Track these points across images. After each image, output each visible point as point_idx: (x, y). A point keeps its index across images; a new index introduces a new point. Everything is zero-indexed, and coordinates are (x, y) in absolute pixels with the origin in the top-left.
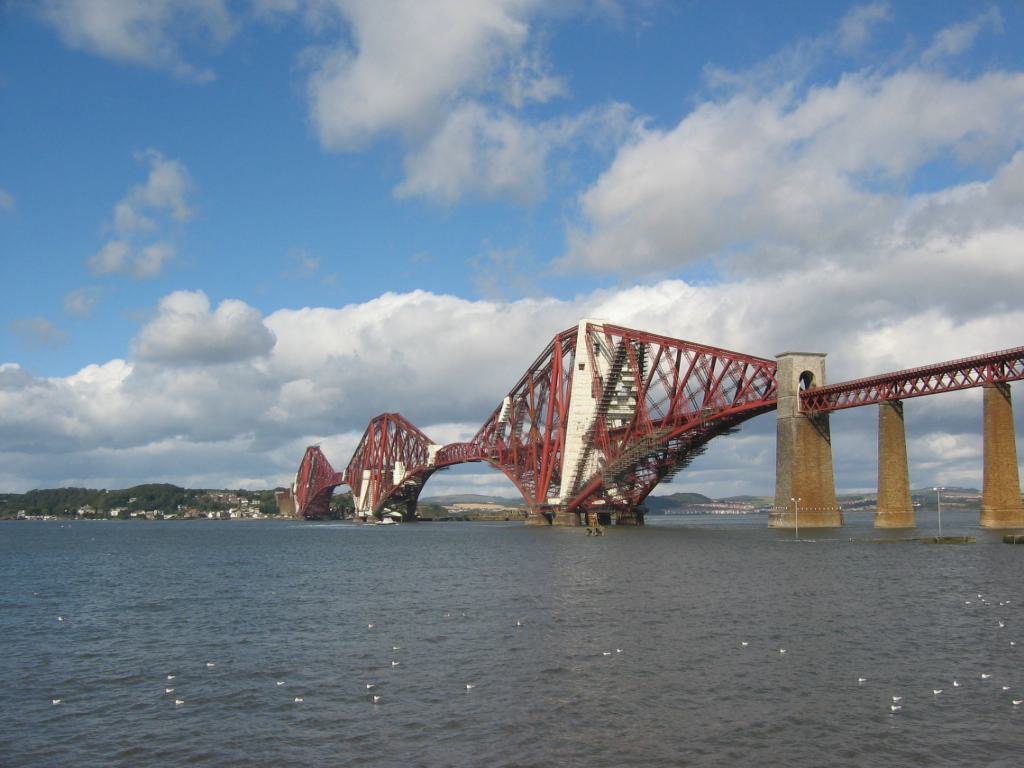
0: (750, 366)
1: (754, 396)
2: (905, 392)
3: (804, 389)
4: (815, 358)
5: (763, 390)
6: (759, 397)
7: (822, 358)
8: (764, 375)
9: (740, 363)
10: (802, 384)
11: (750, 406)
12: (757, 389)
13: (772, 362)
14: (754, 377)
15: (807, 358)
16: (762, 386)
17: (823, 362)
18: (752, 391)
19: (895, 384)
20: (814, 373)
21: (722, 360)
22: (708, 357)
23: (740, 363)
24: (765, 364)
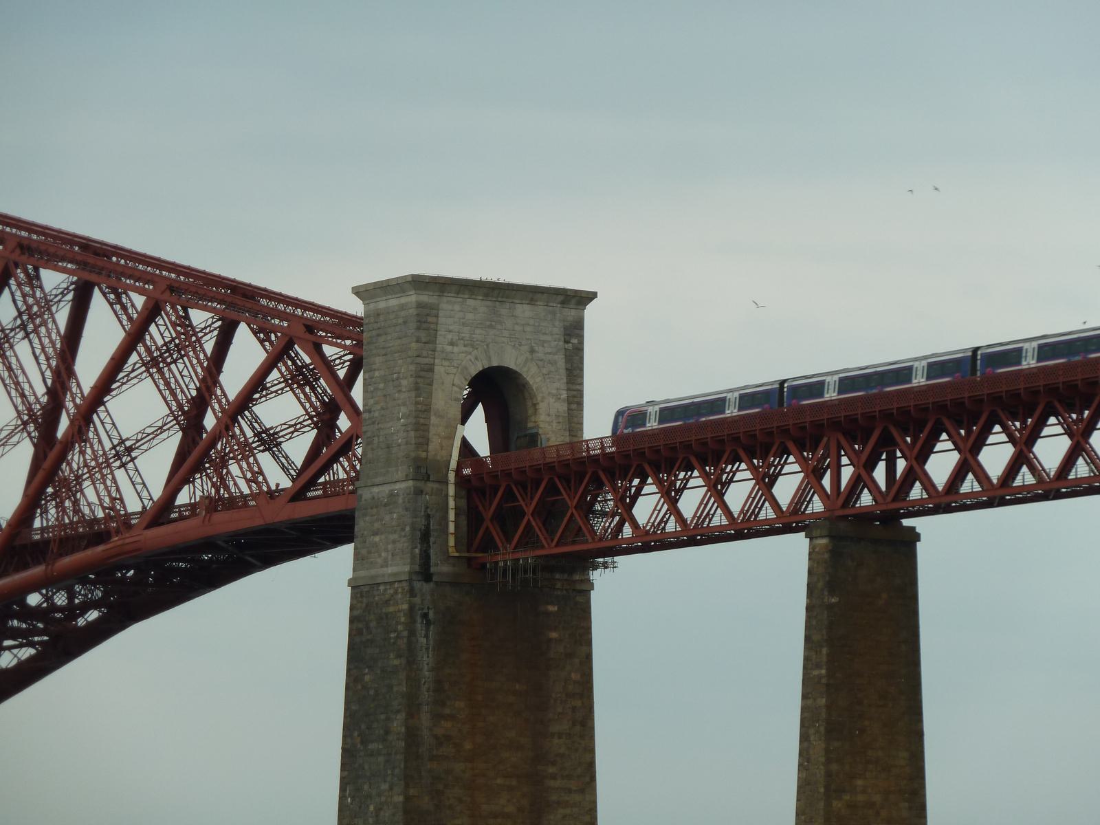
0: (243, 333)
1: (256, 475)
2: (928, 484)
3: (482, 447)
4: (541, 309)
5: (298, 448)
6: (277, 478)
7: (571, 314)
8: (300, 379)
9: (199, 317)
10: (477, 431)
11: (225, 522)
12: (270, 440)
13: (342, 324)
14: (257, 385)
15: (504, 311)
16: (296, 428)
17: (574, 331)
18: (246, 451)
19: (886, 446)
20: (532, 375)
21: (117, 299)
22: (53, 279)
23: (199, 317)
24: (310, 328)
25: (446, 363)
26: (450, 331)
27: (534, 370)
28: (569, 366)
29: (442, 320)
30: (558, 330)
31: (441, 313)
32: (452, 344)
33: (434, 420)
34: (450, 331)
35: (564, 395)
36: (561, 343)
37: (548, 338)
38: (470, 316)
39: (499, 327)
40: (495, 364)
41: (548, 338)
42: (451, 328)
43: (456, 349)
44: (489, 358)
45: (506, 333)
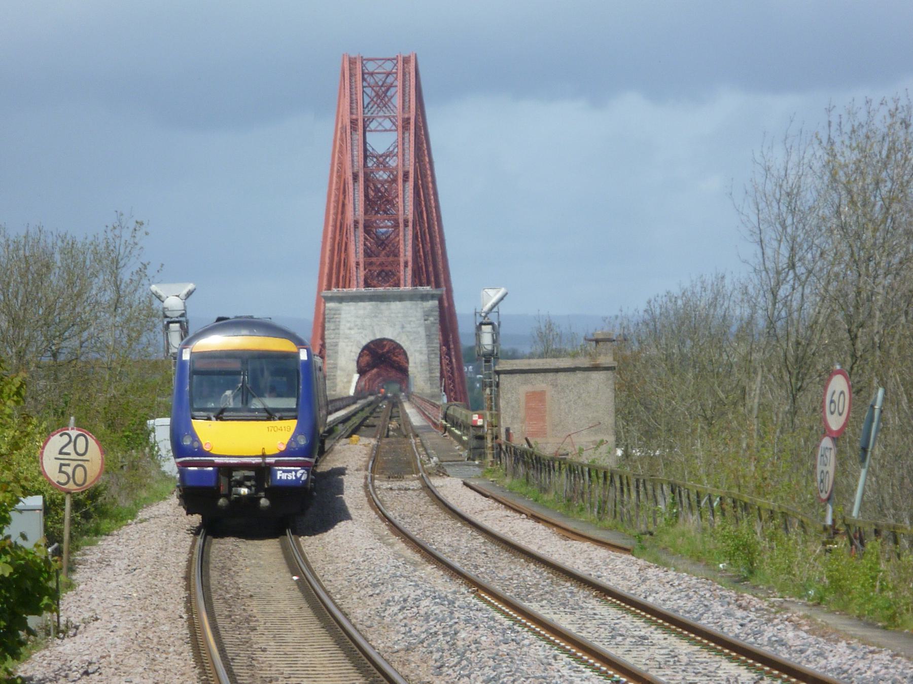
4: (408, 304)
15: (383, 306)
25: (347, 340)
26: (349, 322)
27: (404, 338)
28: (428, 333)
29: (343, 316)
30: (419, 314)
31: (343, 312)
32: (350, 329)
33: (339, 373)
34: (349, 322)
35: (425, 350)
36: (422, 321)
37: (414, 319)
38: (361, 312)
39: (380, 316)
40: (378, 337)
41: (414, 319)
42: (349, 319)
43: (353, 332)
44: (374, 334)
45: (386, 319)
